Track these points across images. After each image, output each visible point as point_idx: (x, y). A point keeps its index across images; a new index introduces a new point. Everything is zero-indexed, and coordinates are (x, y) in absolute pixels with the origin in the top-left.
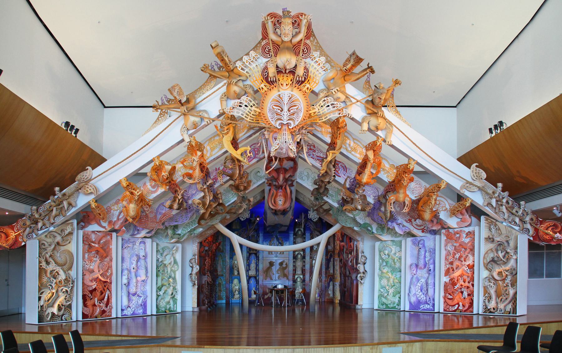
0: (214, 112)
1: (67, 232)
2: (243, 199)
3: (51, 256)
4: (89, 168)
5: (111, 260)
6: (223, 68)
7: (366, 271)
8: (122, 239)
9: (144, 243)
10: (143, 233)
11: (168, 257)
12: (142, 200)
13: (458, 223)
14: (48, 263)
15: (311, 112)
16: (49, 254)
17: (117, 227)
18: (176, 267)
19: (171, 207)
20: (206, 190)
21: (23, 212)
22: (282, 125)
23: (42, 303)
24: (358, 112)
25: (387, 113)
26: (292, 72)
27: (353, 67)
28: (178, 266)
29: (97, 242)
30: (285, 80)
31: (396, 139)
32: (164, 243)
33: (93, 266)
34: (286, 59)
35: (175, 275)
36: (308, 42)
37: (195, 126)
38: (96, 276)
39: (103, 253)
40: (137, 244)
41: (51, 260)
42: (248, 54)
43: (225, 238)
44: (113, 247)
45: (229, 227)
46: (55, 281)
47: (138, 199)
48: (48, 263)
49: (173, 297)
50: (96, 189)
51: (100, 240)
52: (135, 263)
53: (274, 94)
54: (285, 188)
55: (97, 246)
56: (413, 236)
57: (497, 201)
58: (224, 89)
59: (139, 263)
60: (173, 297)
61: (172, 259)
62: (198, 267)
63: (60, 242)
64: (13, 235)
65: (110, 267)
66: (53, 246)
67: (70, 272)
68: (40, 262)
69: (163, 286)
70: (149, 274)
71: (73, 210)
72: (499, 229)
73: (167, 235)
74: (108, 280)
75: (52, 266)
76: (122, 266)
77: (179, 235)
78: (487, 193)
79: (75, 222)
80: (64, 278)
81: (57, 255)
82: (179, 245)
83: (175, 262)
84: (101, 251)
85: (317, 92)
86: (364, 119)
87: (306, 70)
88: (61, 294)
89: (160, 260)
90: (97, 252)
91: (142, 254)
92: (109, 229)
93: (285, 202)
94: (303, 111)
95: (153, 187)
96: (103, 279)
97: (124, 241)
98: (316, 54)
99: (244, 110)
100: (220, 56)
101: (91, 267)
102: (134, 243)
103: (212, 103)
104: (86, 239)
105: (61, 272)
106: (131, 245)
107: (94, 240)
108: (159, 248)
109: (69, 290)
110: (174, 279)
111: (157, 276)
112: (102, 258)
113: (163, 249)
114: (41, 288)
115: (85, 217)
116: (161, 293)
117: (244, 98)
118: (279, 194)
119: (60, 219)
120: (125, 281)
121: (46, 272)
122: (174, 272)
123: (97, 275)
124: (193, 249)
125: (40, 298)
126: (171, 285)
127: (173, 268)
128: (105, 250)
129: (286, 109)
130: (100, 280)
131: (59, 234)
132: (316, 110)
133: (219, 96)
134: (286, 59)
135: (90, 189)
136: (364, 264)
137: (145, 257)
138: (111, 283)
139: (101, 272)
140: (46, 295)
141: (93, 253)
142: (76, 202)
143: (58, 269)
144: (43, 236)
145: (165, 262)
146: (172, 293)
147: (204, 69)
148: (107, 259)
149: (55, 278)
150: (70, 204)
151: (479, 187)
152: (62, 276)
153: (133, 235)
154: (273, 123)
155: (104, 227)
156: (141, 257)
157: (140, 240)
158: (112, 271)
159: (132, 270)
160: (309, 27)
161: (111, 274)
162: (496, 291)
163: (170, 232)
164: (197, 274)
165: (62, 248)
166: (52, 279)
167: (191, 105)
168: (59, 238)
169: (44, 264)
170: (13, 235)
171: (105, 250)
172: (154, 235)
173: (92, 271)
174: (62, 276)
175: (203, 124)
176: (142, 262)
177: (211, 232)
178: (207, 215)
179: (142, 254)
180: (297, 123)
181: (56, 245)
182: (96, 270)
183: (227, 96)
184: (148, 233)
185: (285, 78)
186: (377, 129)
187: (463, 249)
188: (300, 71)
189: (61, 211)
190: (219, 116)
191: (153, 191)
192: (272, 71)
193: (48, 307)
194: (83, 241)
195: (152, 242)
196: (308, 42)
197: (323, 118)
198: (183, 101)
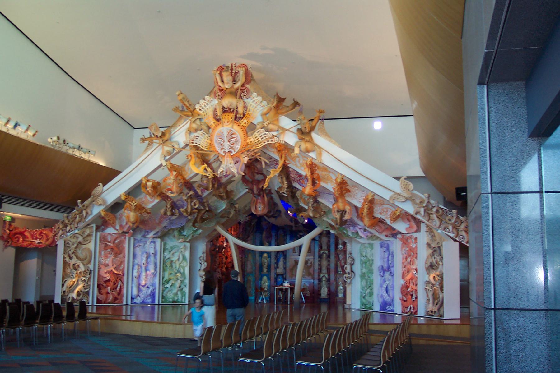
1: (86, 234)
3: (73, 253)
4: (100, 184)
5: (124, 257)
6: (187, 110)
7: (352, 271)
8: (135, 239)
9: (154, 242)
10: (151, 235)
11: (176, 255)
13: (407, 229)
14: (71, 258)
15: (248, 141)
16: (72, 251)
17: (125, 230)
19: (165, 213)
20: (189, 200)
21: (57, 218)
22: (224, 152)
23: (64, 289)
29: (112, 242)
30: (230, 117)
33: (109, 261)
34: (227, 102)
35: (184, 270)
37: (169, 153)
38: (110, 269)
39: (117, 250)
41: (73, 255)
44: (126, 246)
46: (75, 272)
47: (135, 209)
48: (71, 258)
49: (182, 290)
50: (104, 201)
51: (115, 240)
52: (144, 259)
53: (220, 128)
54: (263, 196)
55: (111, 245)
56: (381, 239)
57: (425, 210)
59: (149, 259)
60: (181, 289)
61: (181, 256)
62: (206, 264)
65: (122, 262)
66: (75, 245)
67: (89, 265)
68: (64, 258)
69: (170, 279)
70: (158, 269)
72: (435, 236)
73: (174, 236)
74: (121, 273)
75: (74, 261)
76: (133, 262)
78: (417, 204)
80: (83, 270)
81: (79, 252)
83: (184, 258)
84: (116, 249)
85: (256, 124)
87: (245, 107)
88: (80, 282)
90: (112, 249)
92: (121, 232)
93: (264, 208)
94: (240, 141)
95: (151, 199)
96: (116, 272)
97: (136, 241)
99: (202, 141)
101: (107, 262)
102: (145, 243)
103: (180, 136)
104: (103, 239)
105: (81, 266)
106: (142, 244)
108: (168, 247)
109: (86, 279)
110: (183, 274)
111: (164, 271)
112: (116, 255)
113: (172, 248)
114: (65, 276)
116: (168, 285)
117: (200, 132)
118: (259, 201)
119: (82, 224)
120: (135, 274)
121: (69, 265)
122: (184, 268)
123: (111, 268)
124: (202, 248)
125: (63, 285)
126: (179, 279)
127: (182, 264)
128: (119, 248)
129: (226, 140)
130: (114, 273)
132: (252, 140)
133: (185, 132)
135: (100, 201)
136: (352, 265)
137: (155, 254)
138: (123, 275)
139: (115, 266)
140: (69, 282)
141: (109, 250)
142: (91, 212)
143: (79, 263)
144: (68, 237)
145: (173, 259)
146: (180, 287)
148: (121, 256)
149: (76, 270)
150: (87, 213)
151: (406, 198)
152: (82, 268)
153: (144, 236)
154: (219, 151)
155: (117, 230)
156: (151, 254)
157: (150, 240)
158: (124, 265)
159: (143, 266)
161: (124, 268)
162: (433, 295)
163: (176, 233)
164: (204, 270)
165: (84, 246)
166: (74, 270)
167: (165, 138)
168: (80, 239)
169: (67, 259)
171: (119, 248)
173: (107, 265)
174: (82, 268)
175: (175, 152)
176: (152, 259)
178: (199, 219)
179: (152, 251)
180: (237, 151)
181: (78, 245)
182: (111, 264)
183: (190, 131)
185: (226, 117)
187: (412, 254)
190: (187, 145)
191: (151, 202)
193: (70, 292)
194: (100, 240)
197: (259, 145)
198: (159, 136)
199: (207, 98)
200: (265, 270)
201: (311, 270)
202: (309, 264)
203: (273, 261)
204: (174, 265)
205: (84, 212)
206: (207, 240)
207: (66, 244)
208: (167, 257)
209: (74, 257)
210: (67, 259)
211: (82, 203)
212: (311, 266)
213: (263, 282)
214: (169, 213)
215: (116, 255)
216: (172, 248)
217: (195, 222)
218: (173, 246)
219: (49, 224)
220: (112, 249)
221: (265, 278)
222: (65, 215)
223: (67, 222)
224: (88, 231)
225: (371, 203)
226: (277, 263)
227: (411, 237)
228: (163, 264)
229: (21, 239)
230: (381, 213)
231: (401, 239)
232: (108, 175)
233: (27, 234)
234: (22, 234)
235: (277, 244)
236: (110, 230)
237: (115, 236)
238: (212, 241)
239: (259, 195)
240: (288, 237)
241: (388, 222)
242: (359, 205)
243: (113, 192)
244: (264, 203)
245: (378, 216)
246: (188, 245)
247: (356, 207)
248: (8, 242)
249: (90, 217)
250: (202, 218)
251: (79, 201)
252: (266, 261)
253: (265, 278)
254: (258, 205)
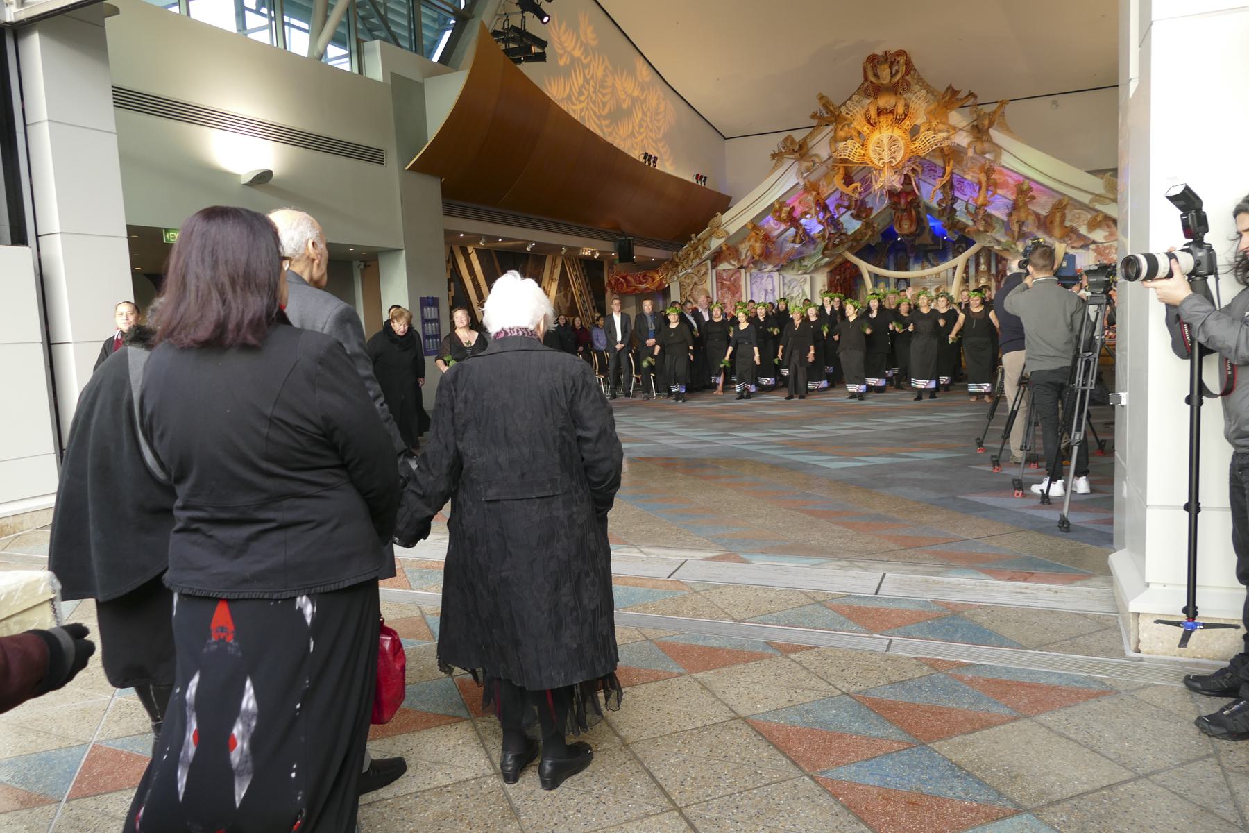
0: (825, 155)
2: (868, 225)
10: (770, 267)
12: (767, 238)
13: (1105, 237)
24: (963, 139)
25: (996, 135)
26: (892, 112)
27: (950, 98)
31: (1007, 160)
32: (790, 275)
36: (908, 78)
37: (808, 169)
42: (850, 98)
43: (856, 267)
44: (743, 283)
45: (857, 254)
50: (727, 233)
53: (876, 136)
58: (832, 134)
64: (658, 279)
71: (708, 253)
79: (709, 262)
82: (808, 277)
86: (969, 145)
91: (770, 288)
98: (917, 88)
100: (826, 106)
104: (719, 277)
112: (733, 294)
115: (717, 258)
134: (884, 101)
135: (720, 232)
137: (773, 291)
147: (814, 116)
160: (908, 63)
167: (804, 151)
168: (696, 279)
170: (658, 279)
172: (781, 269)
177: (839, 260)
179: (770, 288)
183: (835, 140)
186: (984, 153)
188: (900, 110)
189: (697, 254)
192: (873, 113)
196: (908, 78)
199: (856, 98)
205: (700, 248)
206: (828, 270)
207: (681, 285)
215: (733, 294)
217: (826, 248)
219: (654, 266)
225: (1062, 206)
227: (1110, 247)
230: (1071, 220)
231: (1095, 250)
233: (630, 278)
235: (898, 270)
236: (723, 266)
239: (904, 210)
240: (912, 260)
241: (1083, 230)
242: (1043, 213)
244: (911, 221)
245: (1067, 224)
247: (1037, 215)
249: (708, 253)
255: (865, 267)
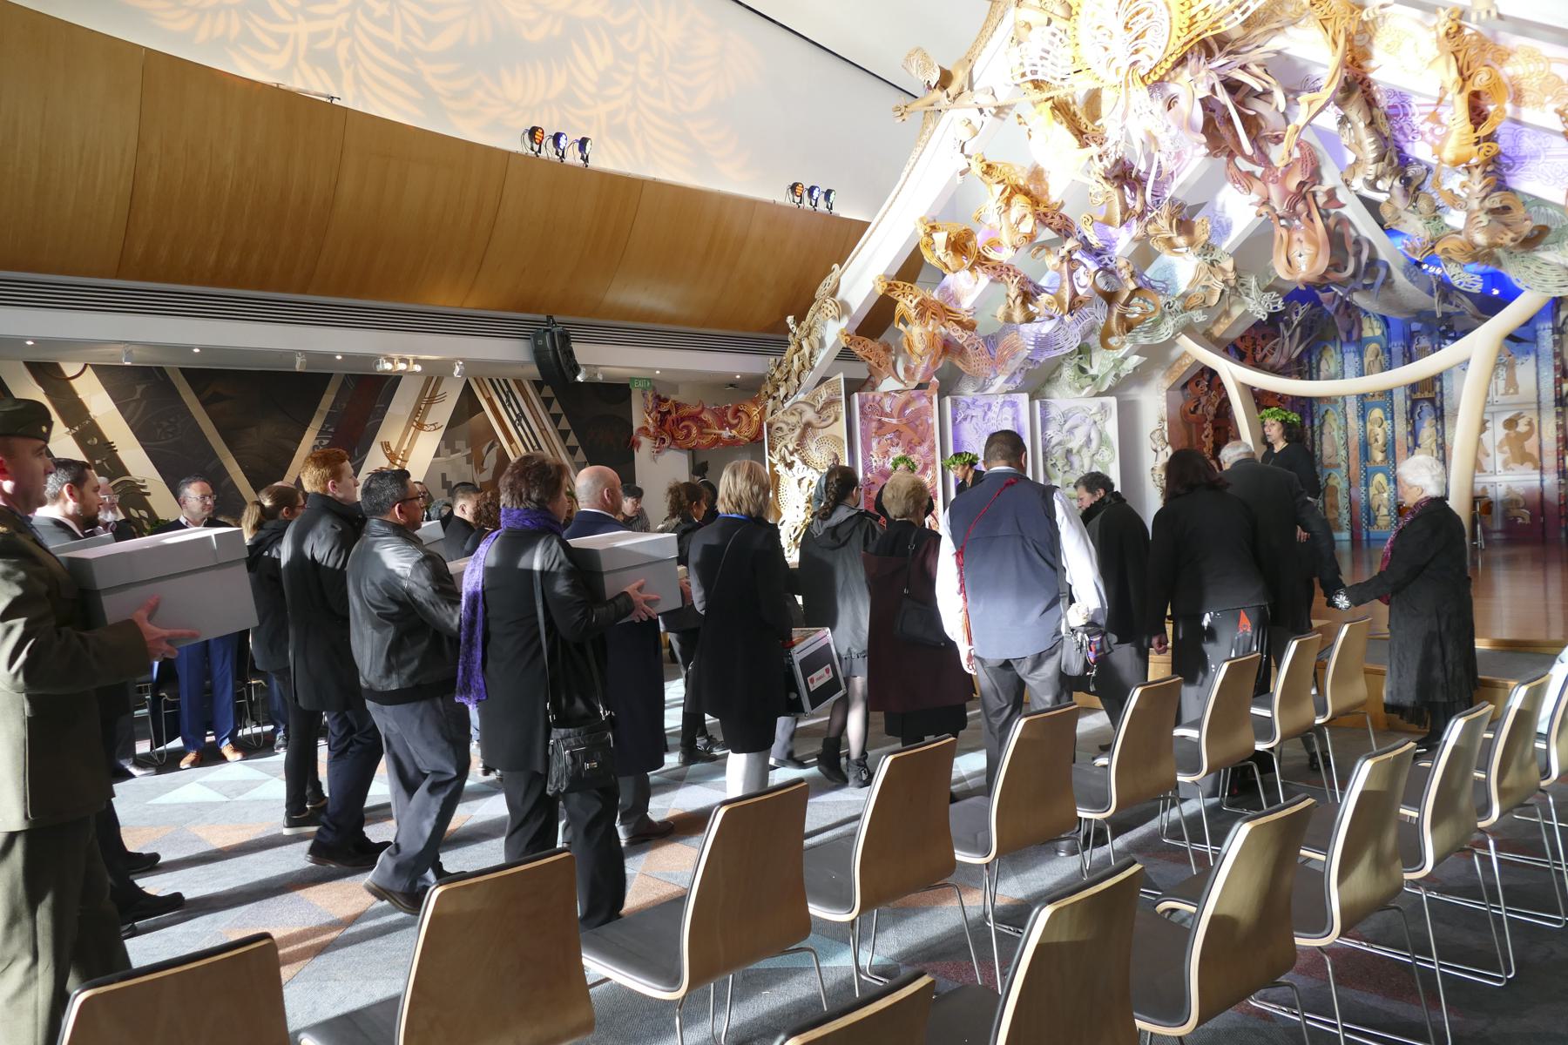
5: (932, 449)
8: (955, 404)
9: (1014, 404)
14: (790, 466)
18: (1107, 453)
28: (1113, 452)
40: (995, 409)
41: (796, 458)
47: (921, 315)
48: (790, 466)
50: (844, 308)
55: (894, 421)
63: (815, 422)
66: (798, 431)
77: (1094, 378)
82: (1112, 401)
83: (1103, 441)
89: (1054, 442)
90: (898, 433)
106: (978, 412)
107: (888, 410)
108: (1054, 412)
113: (1066, 417)
119: (809, 378)
131: (813, 406)
145: (1069, 446)
148: (924, 449)
153: (982, 389)
157: (1001, 399)
165: (821, 433)
167: (952, 90)
168: (809, 415)
169: (780, 468)
171: (915, 430)
184: (1007, 382)
194: (862, 413)
195: (1032, 399)
200: (1379, 456)
201: (1531, 445)
202: (1522, 427)
203: (1401, 428)
204: (1075, 459)
206: (1167, 384)
208: (1054, 442)
209: (798, 464)
210: (780, 468)
211: (798, 321)
212: (1528, 435)
213: (1372, 491)
214: (1018, 315)
216: (1066, 417)
218: (1070, 410)
219: (751, 388)
220: (898, 433)
221: (1380, 478)
222: (772, 359)
223: (778, 375)
224: (824, 393)
226: (1414, 433)
228: (1045, 459)
229: (694, 431)
232: (844, 238)
233: (706, 416)
234: (695, 418)
237: (903, 398)
238: (1185, 386)
243: (860, 279)
246: (1112, 401)
248: (663, 441)
250: (1122, 317)
251: (790, 319)
252: (1379, 433)
253: (1380, 478)
254: (1296, 249)
255: (1233, 375)
